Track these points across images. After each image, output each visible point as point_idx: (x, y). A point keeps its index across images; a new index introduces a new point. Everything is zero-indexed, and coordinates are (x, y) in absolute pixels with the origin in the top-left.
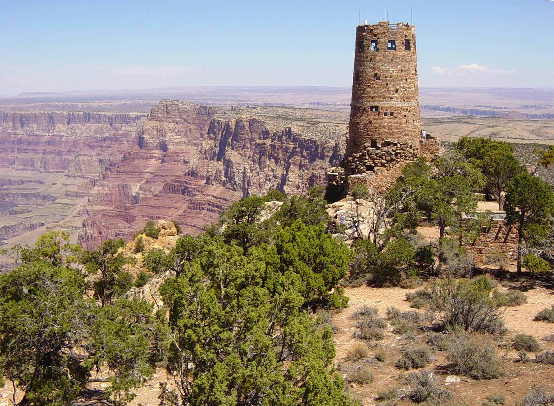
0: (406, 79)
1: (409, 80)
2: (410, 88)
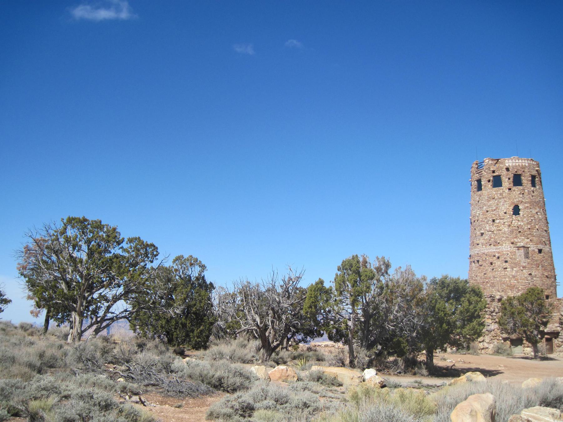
0: (494, 221)
1: (498, 221)
2: (500, 230)
